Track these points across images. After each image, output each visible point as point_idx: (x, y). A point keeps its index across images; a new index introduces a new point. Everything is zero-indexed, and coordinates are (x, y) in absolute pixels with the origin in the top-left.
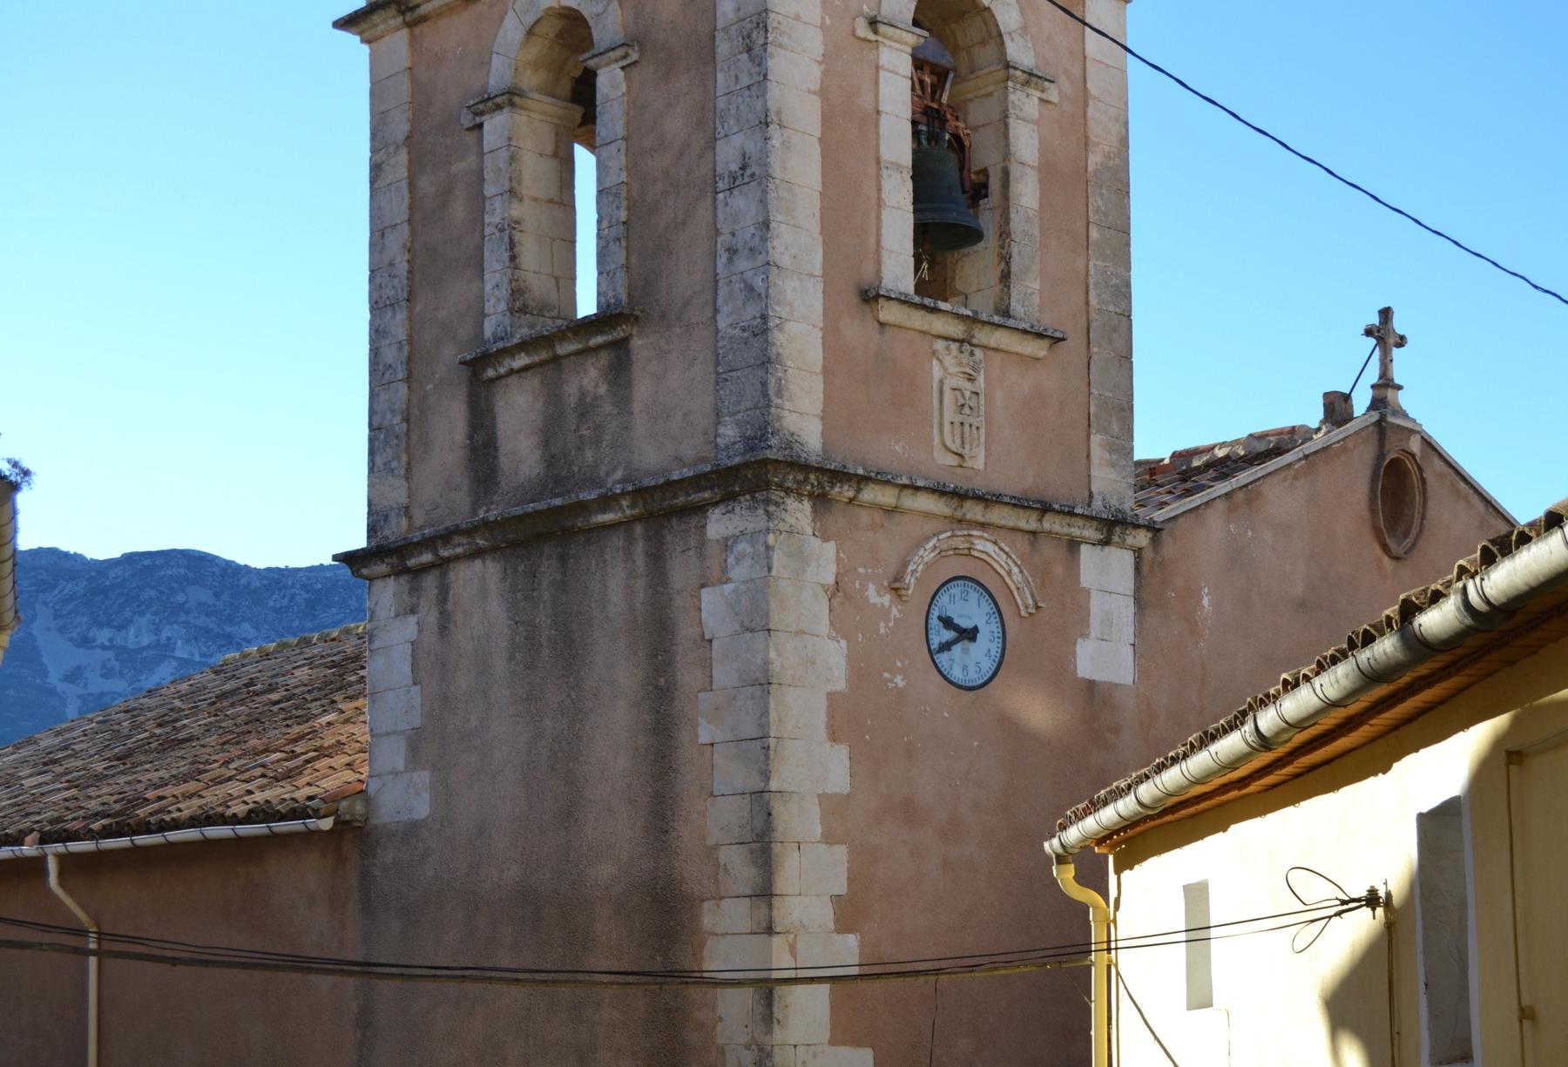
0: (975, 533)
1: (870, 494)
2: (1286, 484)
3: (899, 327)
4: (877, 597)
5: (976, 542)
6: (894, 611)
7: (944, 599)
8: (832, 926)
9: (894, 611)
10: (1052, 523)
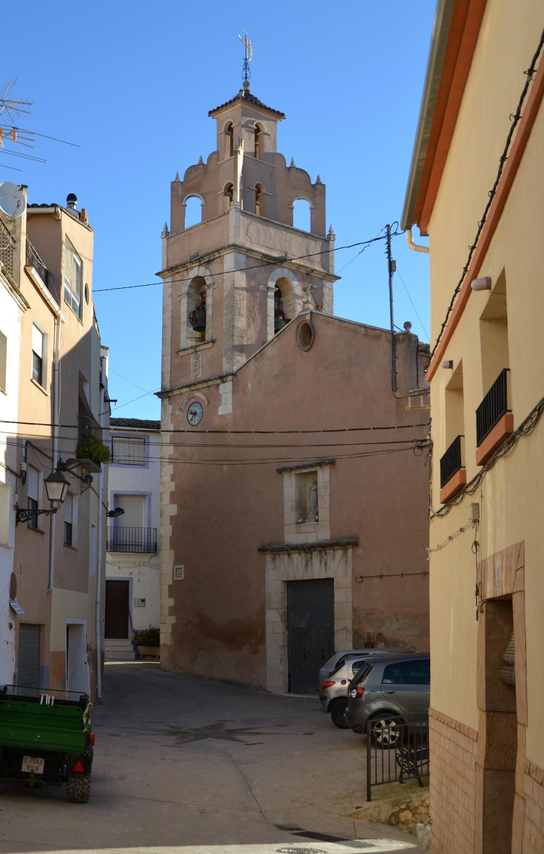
0: (193, 392)
1: (175, 393)
2: (272, 346)
3: (183, 356)
4: (178, 413)
5: (195, 394)
6: (181, 414)
7: (191, 408)
8: (170, 481)
9: (181, 414)
10: (210, 383)
